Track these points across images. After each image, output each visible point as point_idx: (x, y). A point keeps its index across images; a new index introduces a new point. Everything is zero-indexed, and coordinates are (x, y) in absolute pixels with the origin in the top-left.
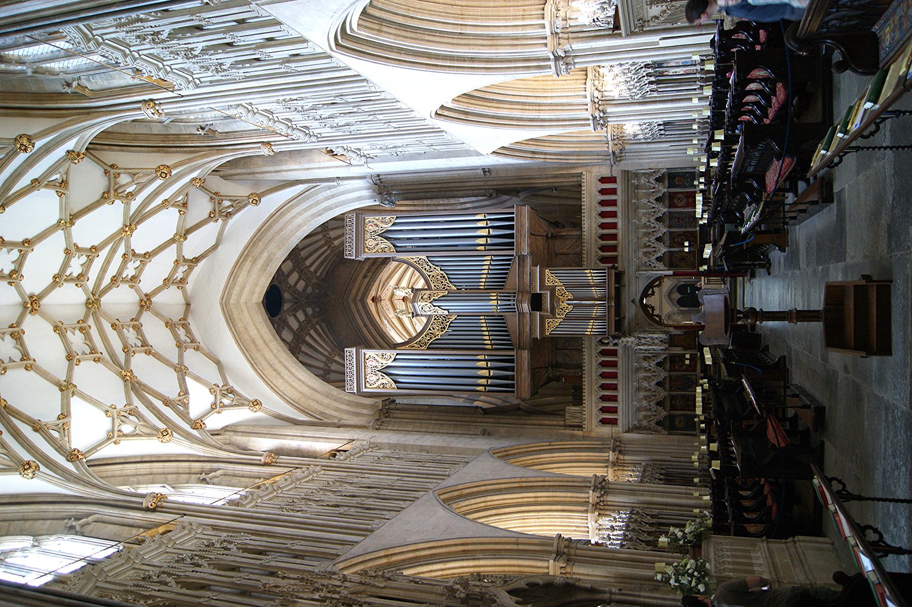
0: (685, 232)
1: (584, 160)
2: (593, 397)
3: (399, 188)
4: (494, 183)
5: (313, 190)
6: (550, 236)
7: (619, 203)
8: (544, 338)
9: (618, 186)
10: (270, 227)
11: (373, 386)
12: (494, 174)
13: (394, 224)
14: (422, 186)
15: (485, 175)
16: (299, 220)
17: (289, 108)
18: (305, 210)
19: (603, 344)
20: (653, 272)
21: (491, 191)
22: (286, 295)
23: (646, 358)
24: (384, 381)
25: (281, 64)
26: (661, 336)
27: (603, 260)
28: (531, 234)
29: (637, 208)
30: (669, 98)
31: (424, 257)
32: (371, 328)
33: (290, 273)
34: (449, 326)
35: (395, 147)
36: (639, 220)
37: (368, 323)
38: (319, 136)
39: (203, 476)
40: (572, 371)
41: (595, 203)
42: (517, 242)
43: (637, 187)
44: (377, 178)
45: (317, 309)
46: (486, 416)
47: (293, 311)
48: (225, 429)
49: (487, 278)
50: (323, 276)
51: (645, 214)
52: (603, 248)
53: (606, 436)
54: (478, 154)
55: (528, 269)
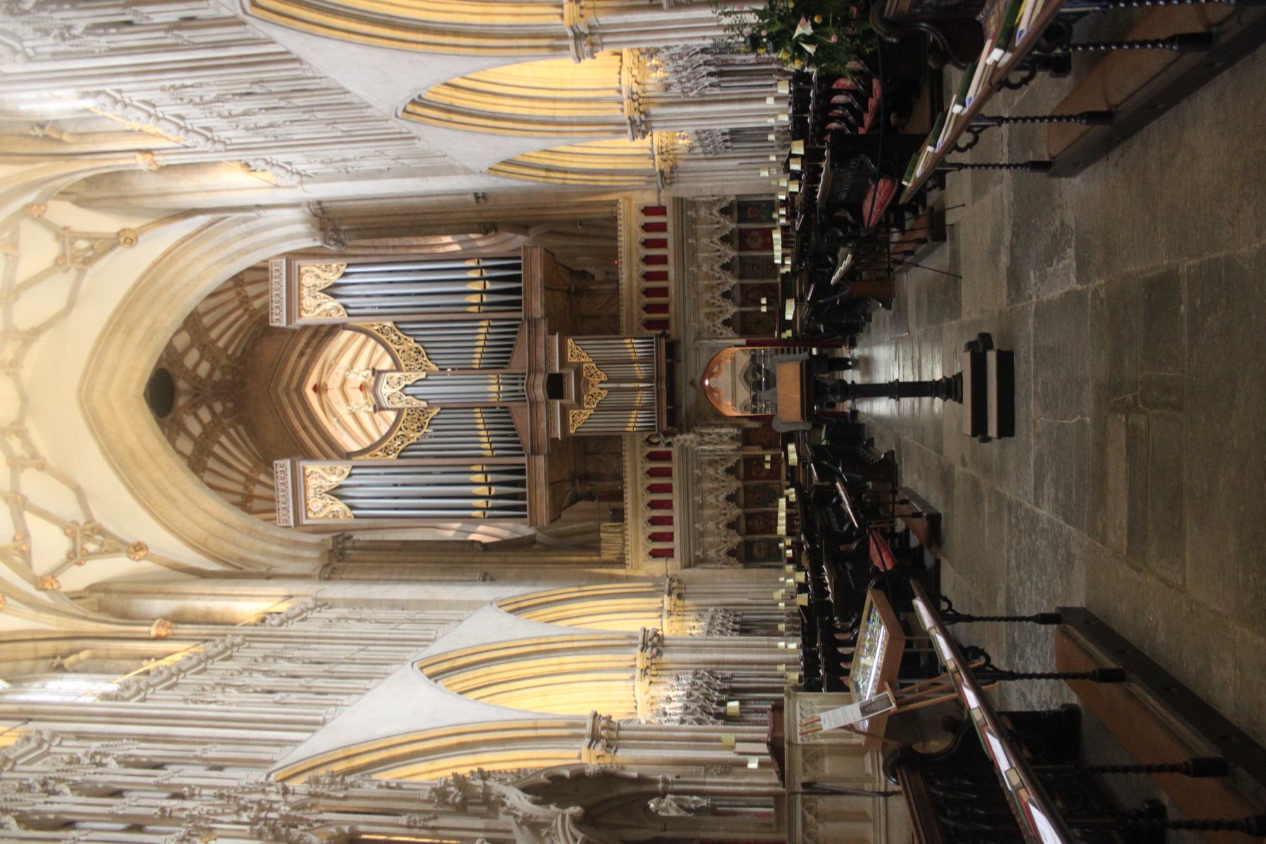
0: (763, 284)
4: (492, 214)
5: (219, 224)
6: (573, 290)
7: (670, 244)
8: (567, 439)
9: (669, 219)
11: (317, 515)
13: (345, 275)
15: (477, 202)
16: (199, 268)
17: (181, 99)
19: (651, 444)
20: (719, 341)
22: (182, 384)
23: (711, 463)
25: (167, 31)
26: (731, 430)
27: (649, 325)
28: (546, 288)
30: (736, 97)
31: (389, 324)
32: (314, 431)
33: (187, 350)
34: (429, 425)
35: (344, 160)
36: (699, 267)
37: (308, 423)
38: (228, 142)
39: (57, 661)
40: (608, 484)
41: (636, 244)
43: (695, 221)
44: (318, 206)
45: (230, 405)
46: (487, 553)
47: (193, 408)
48: (92, 589)
50: (238, 354)
51: (706, 260)
52: (649, 308)
53: (658, 574)
54: (468, 171)
55: (541, 340)
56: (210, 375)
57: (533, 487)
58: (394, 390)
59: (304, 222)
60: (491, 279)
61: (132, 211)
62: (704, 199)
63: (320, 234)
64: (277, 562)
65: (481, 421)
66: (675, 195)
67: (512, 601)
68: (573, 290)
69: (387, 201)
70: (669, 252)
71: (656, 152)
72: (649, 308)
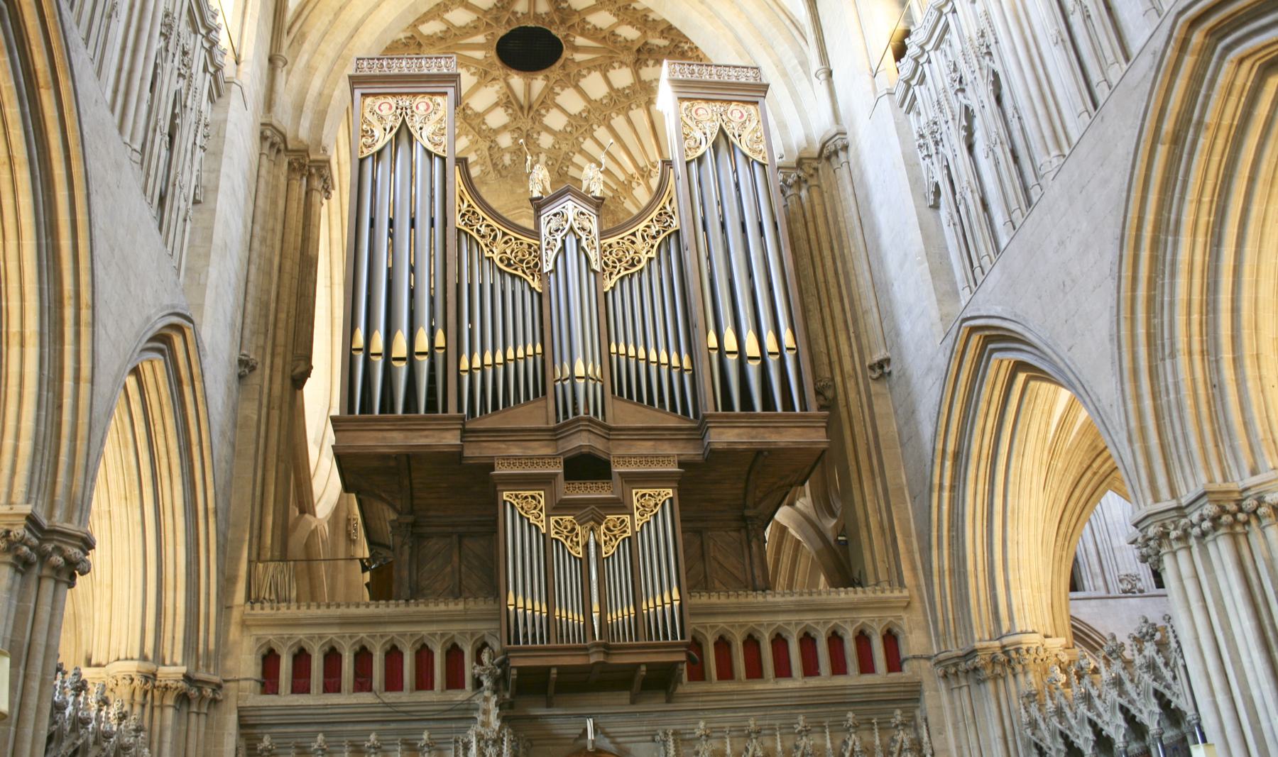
2: (336, 630)
3: (816, 200)
14: (825, 245)
15: (872, 367)
19: (478, 652)
21: (829, 394)
22: (539, 83)
24: (378, 132)
28: (758, 453)
29: (839, 727)
31: (675, 224)
34: (513, 276)
40: (405, 573)
42: (738, 416)
44: (839, 143)
46: (288, 382)
53: (230, 663)
55: (667, 449)
56: (548, 129)
57: (401, 425)
58: (571, 219)
59: (808, 140)
62: (926, 739)
63: (792, 161)
64: (295, 81)
65: (520, 354)
67: (196, 370)
70: (825, 678)
72: (723, 645)
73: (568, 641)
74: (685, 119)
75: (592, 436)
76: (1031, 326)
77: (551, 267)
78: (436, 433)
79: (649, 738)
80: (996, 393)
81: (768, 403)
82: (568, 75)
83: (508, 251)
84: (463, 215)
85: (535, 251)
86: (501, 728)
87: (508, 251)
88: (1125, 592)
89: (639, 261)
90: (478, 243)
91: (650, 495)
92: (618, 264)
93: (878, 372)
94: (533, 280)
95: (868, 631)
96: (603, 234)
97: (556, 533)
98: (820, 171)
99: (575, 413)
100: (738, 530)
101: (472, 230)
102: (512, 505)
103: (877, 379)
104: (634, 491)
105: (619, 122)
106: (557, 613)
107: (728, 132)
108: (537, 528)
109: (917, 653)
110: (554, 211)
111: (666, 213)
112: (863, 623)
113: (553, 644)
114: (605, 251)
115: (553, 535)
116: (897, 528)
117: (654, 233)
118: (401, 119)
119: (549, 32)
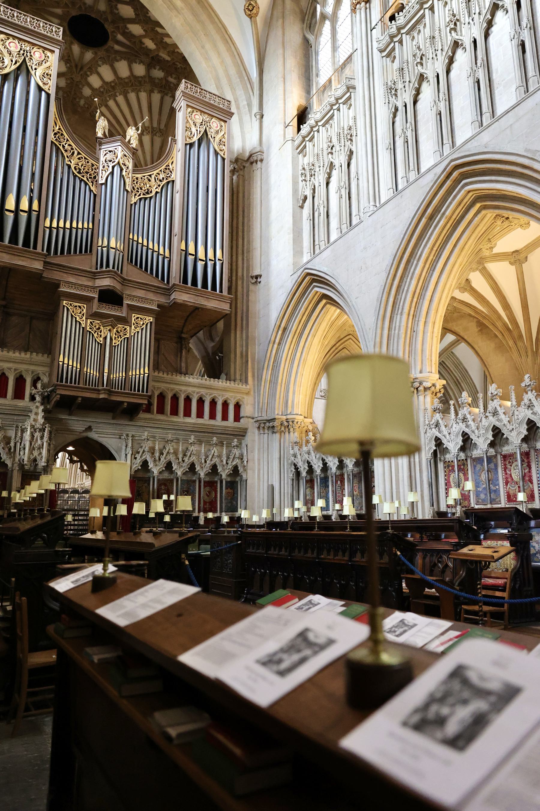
1: (265, 387)
3: (241, 183)
5: (249, 86)
7: (212, 422)
10: (213, 22)
12: (252, 287)
13: (216, 153)
15: (252, 277)
18: (226, 71)
22: (89, 55)
24: (7, 61)
26: (44, 460)
28: (197, 309)
29: (208, 443)
34: (81, 180)
42: (189, 288)
43: (229, 445)
44: (259, 158)
49: (143, 246)
55: (151, 296)
58: (119, 157)
60: (206, 267)
61: (269, 23)
66: (249, 431)
68: (184, 336)
69: (259, 210)
70: (206, 419)
71: (289, 417)
73: (89, 385)
74: (188, 118)
75: (115, 281)
76: (340, 282)
77: (103, 181)
78: (29, 260)
79: (118, 437)
80: (311, 306)
81: (205, 285)
82: (109, 56)
83: (80, 165)
84: (55, 134)
85: (95, 169)
86: (44, 424)
87: (80, 165)
88: (321, 396)
89: (151, 192)
90: (62, 154)
91: (141, 318)
92: (140, 191)
93: (255, 280)
94: (92, 185)
95: (229, 401)
96: (134, 171)
97: (90, 328)
98: (246, 169)
99: (108, 265)
100: (176, 343)
101: (60, 145)
102: (68, 309)
103: (253, 283)
104: (133, 315)
105: (132, 96)
106: (85, 370)
107: (209, 133)
108: (80, 323)
109: (248, 415)
110: (110, 149)
111: (169, 169)
112: (227, 398)
113: (81, 385)
114: (134, 181)
115: (88, 329)
116: (249, 356)
117: (161, 179)
118: (23, 58)
119: (103, 26)
